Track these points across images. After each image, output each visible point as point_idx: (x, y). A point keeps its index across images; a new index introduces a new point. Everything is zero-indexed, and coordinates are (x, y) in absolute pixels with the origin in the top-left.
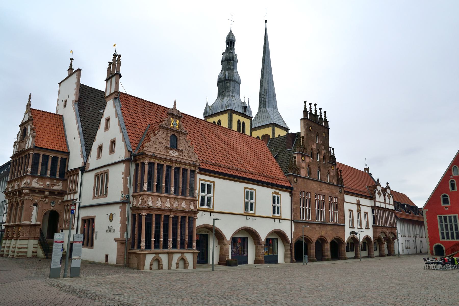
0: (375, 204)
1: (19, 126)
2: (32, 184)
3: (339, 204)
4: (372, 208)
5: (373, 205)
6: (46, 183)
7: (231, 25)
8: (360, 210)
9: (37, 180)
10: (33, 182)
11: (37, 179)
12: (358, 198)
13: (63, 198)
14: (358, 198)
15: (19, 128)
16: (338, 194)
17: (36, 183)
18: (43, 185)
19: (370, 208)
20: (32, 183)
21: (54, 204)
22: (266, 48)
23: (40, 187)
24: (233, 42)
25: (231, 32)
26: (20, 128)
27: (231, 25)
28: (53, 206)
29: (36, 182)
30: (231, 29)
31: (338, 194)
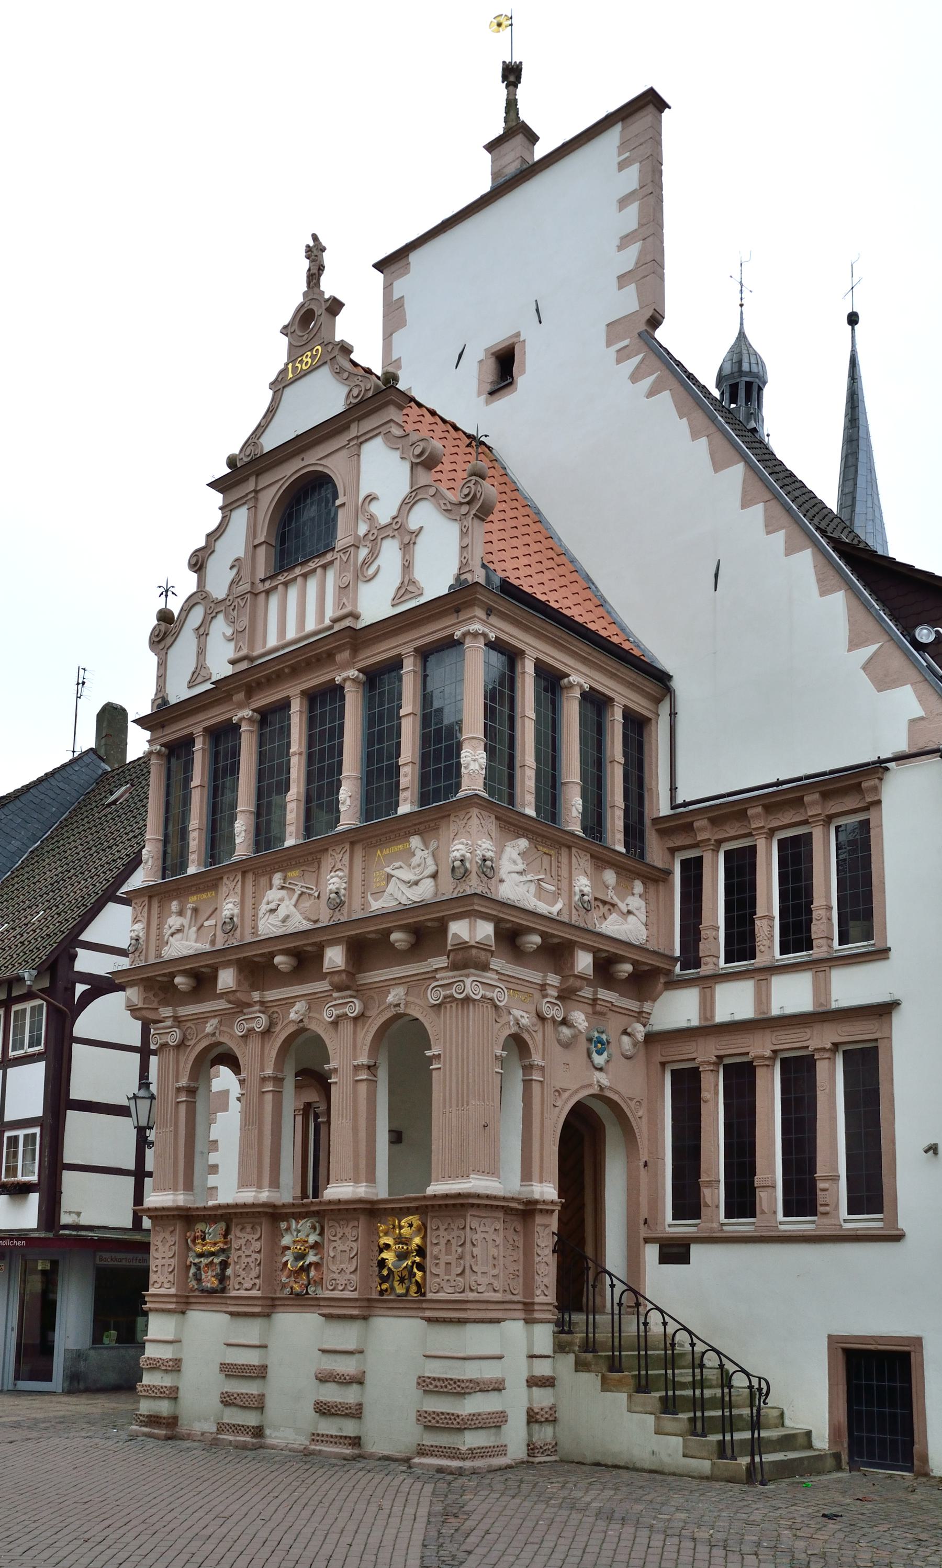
1: (216, 485)
2: (502, 881)
6: (571, 886)
7: (741, 305)
9: (522, 854)
10: (505, 857)
11: (523, 843)
13: (647, 1007)
15: (218, 498)
17: (520, 873)
18: (558, 894)
20: (503, 873)
21: (605, 1054)
22: (857, 440)
23: (542, 908)
24: (759, 386)
25: (742, 336)
26: (221, 504)
27: (741, 305)
28: (601, 1069)
29: (521, 867)
30: (742, 324)
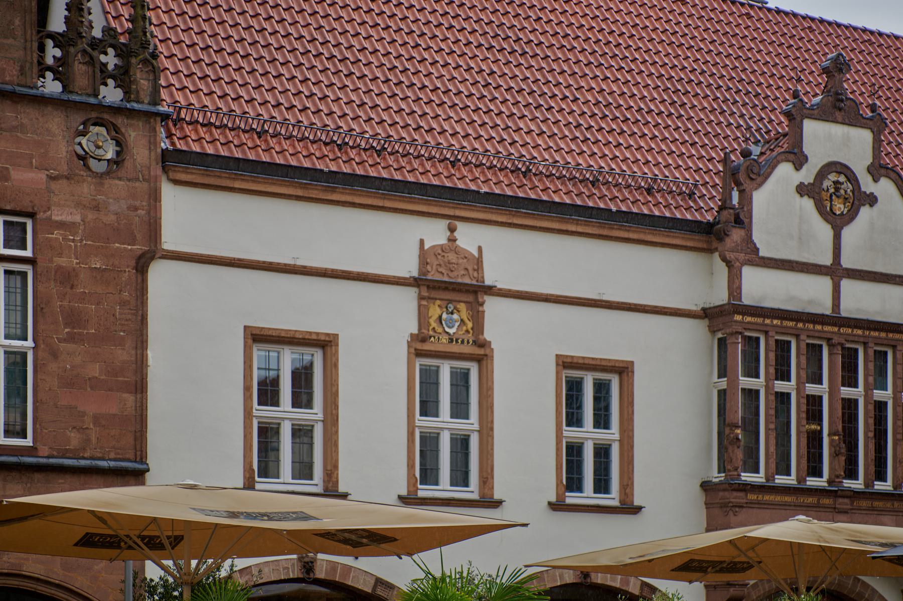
0: (735, 288)
3: (67, 278)
4: (713, 331)
5: (720, 296)
8: (484, 344)
12: (452, 229)
14: (452, 229)
16: (42, 176)
19: (697, 329)
31: (52, 178)
